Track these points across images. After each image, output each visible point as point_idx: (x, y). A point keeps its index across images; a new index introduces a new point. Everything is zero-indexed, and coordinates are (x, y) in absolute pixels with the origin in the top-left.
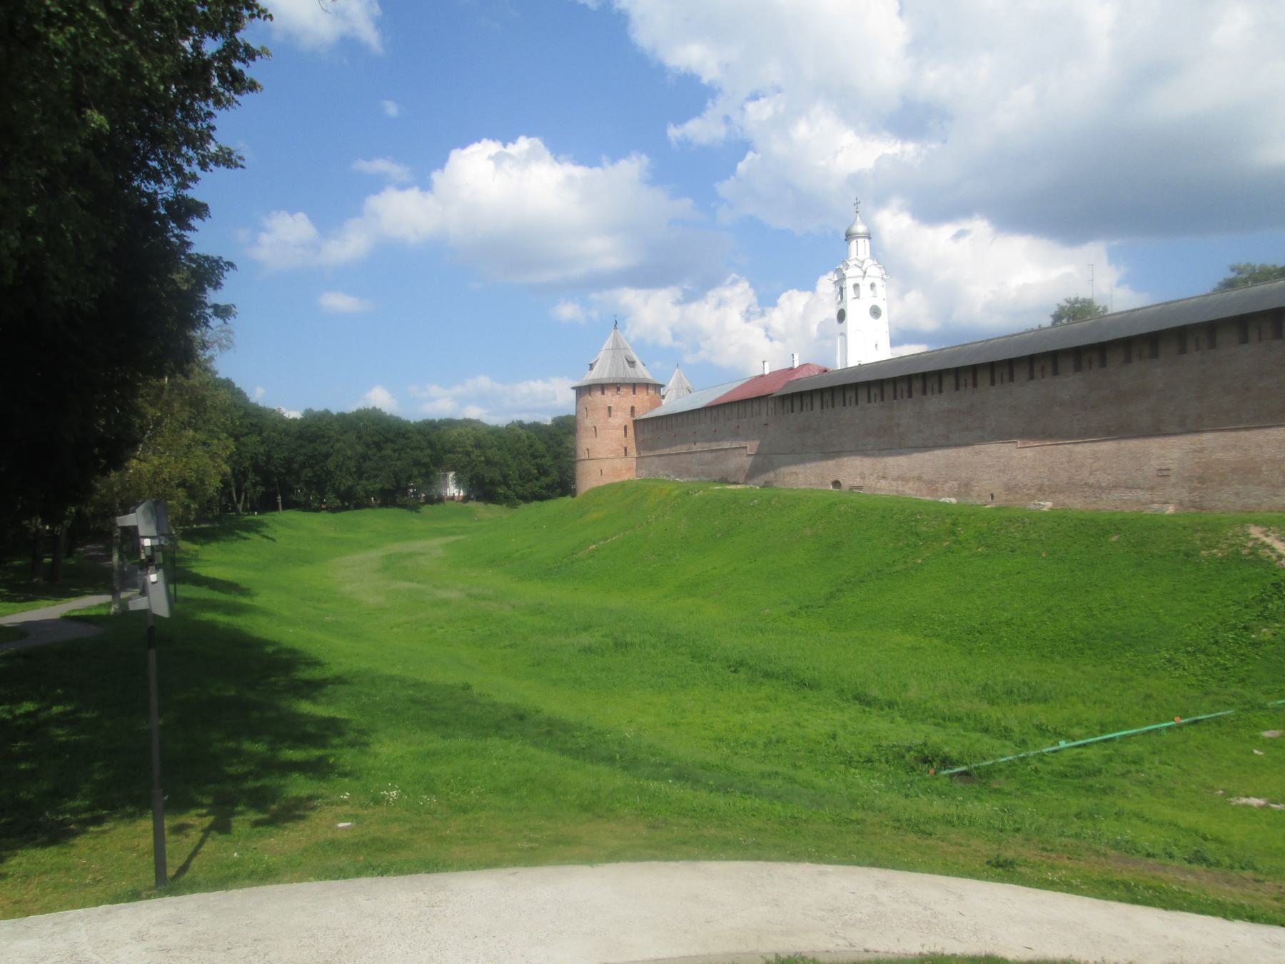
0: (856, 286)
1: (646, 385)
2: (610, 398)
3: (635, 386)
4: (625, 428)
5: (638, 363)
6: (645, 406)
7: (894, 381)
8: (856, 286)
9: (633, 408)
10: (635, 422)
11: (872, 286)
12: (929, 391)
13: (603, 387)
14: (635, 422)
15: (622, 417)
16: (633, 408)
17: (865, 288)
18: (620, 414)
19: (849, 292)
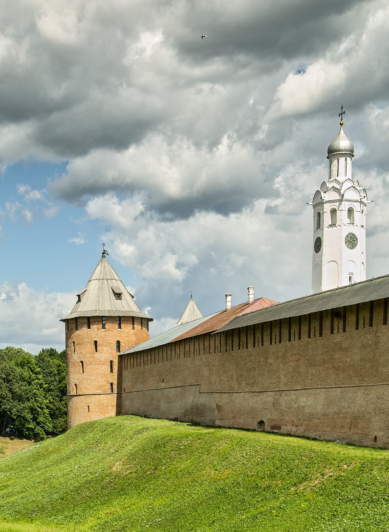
0: (334, 211)
1: (132, 320)
2: (95, 332)
3: (120, 320)
4: (111, 362)
5: (126, 296)
6: (131, 339)
7: (310, 317)
8: (334, 211)
9: (118, 342)
10: (120, 357)
11: (350, 211)
12: (335, 331)
13: (89, 321)
14: (120, 357)
15: (108, 353)
16: (118, 342)
17: (342, 216)
18: (105, 349)
19: (327, 219)
